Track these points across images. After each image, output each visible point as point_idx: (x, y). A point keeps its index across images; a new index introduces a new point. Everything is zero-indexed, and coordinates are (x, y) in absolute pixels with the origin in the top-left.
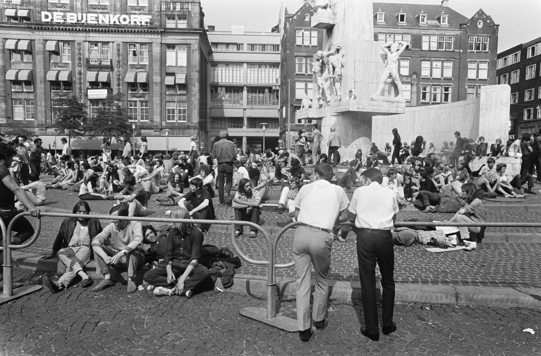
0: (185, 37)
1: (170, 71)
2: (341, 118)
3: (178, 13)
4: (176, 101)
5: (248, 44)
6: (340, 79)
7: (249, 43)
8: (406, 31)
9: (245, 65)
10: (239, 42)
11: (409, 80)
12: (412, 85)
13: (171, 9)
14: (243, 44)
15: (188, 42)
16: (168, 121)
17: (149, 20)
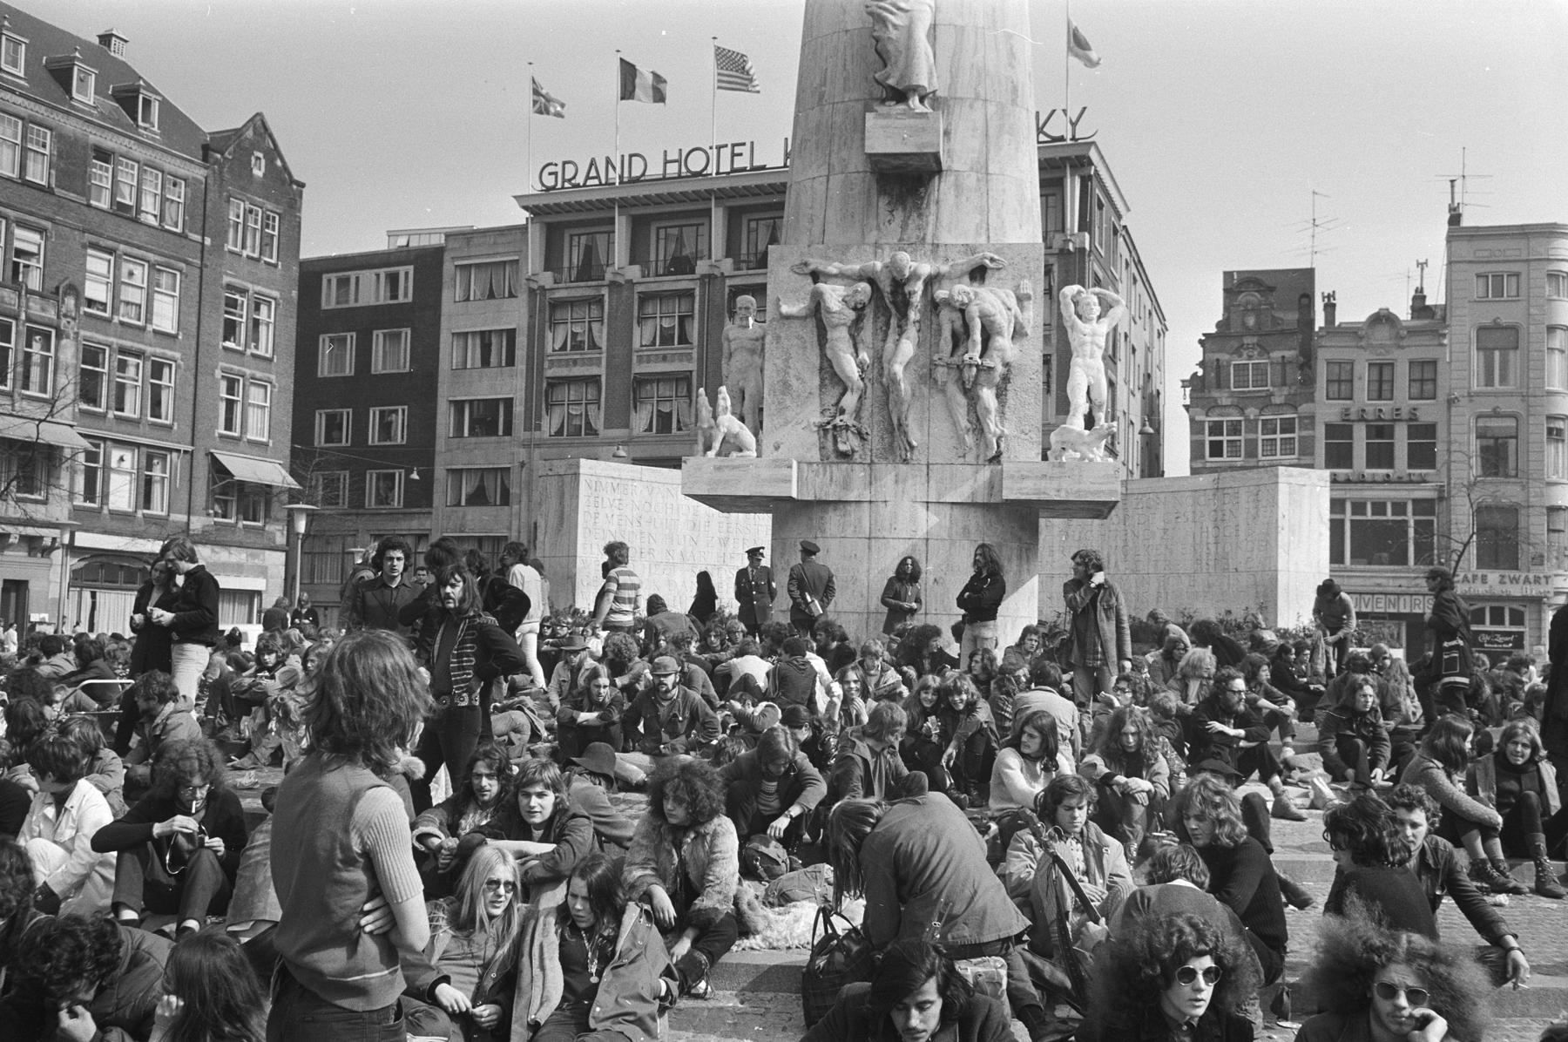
8: (40, 112)
11: (51, 314)
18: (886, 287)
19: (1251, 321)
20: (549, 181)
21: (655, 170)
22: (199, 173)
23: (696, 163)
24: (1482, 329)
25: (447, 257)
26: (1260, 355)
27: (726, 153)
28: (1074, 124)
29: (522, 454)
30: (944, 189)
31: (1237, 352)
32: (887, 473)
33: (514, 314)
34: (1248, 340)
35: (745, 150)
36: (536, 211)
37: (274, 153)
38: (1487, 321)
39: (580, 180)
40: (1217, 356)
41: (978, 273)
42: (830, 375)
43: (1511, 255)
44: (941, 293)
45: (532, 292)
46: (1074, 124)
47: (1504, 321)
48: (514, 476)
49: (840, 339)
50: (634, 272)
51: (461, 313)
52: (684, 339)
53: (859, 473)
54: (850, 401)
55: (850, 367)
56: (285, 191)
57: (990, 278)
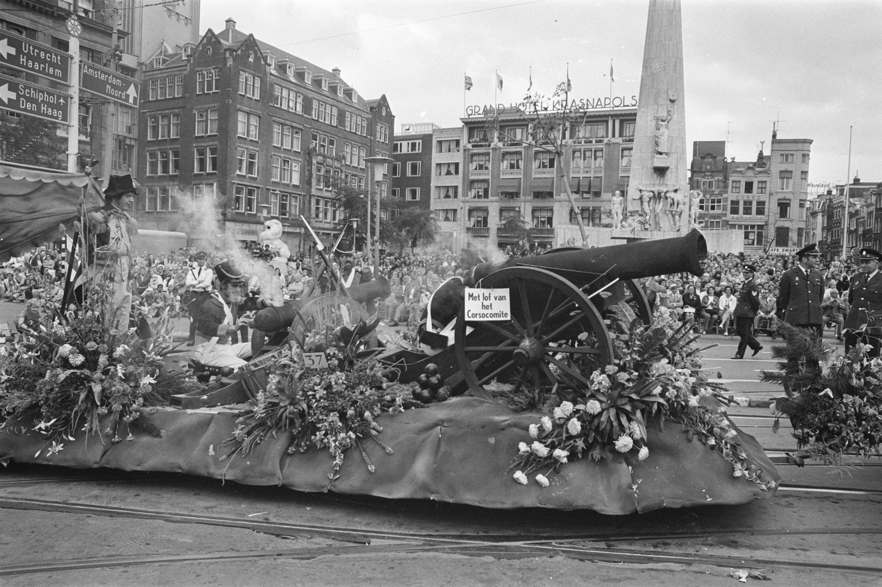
18: (656, 193)
19: (708, 167)
20: (470, 112)
22: (370, 116)
24: (781, 172)
25: (434, 137)
29: (462, 205)
30: (668, 173)
33: (457, 157)
36: (466, 123)
37: (388, 107)
38: (783, 169)
41: (676, 191)
43: (792, 148)
44: (668, 195)
45: (465, 150)
47: (789, 169)
48: (458, 212)
49: (646, 204)
50: (500, 145)
51: (437, 157)
52: (518, 167)
56: (390, 119)
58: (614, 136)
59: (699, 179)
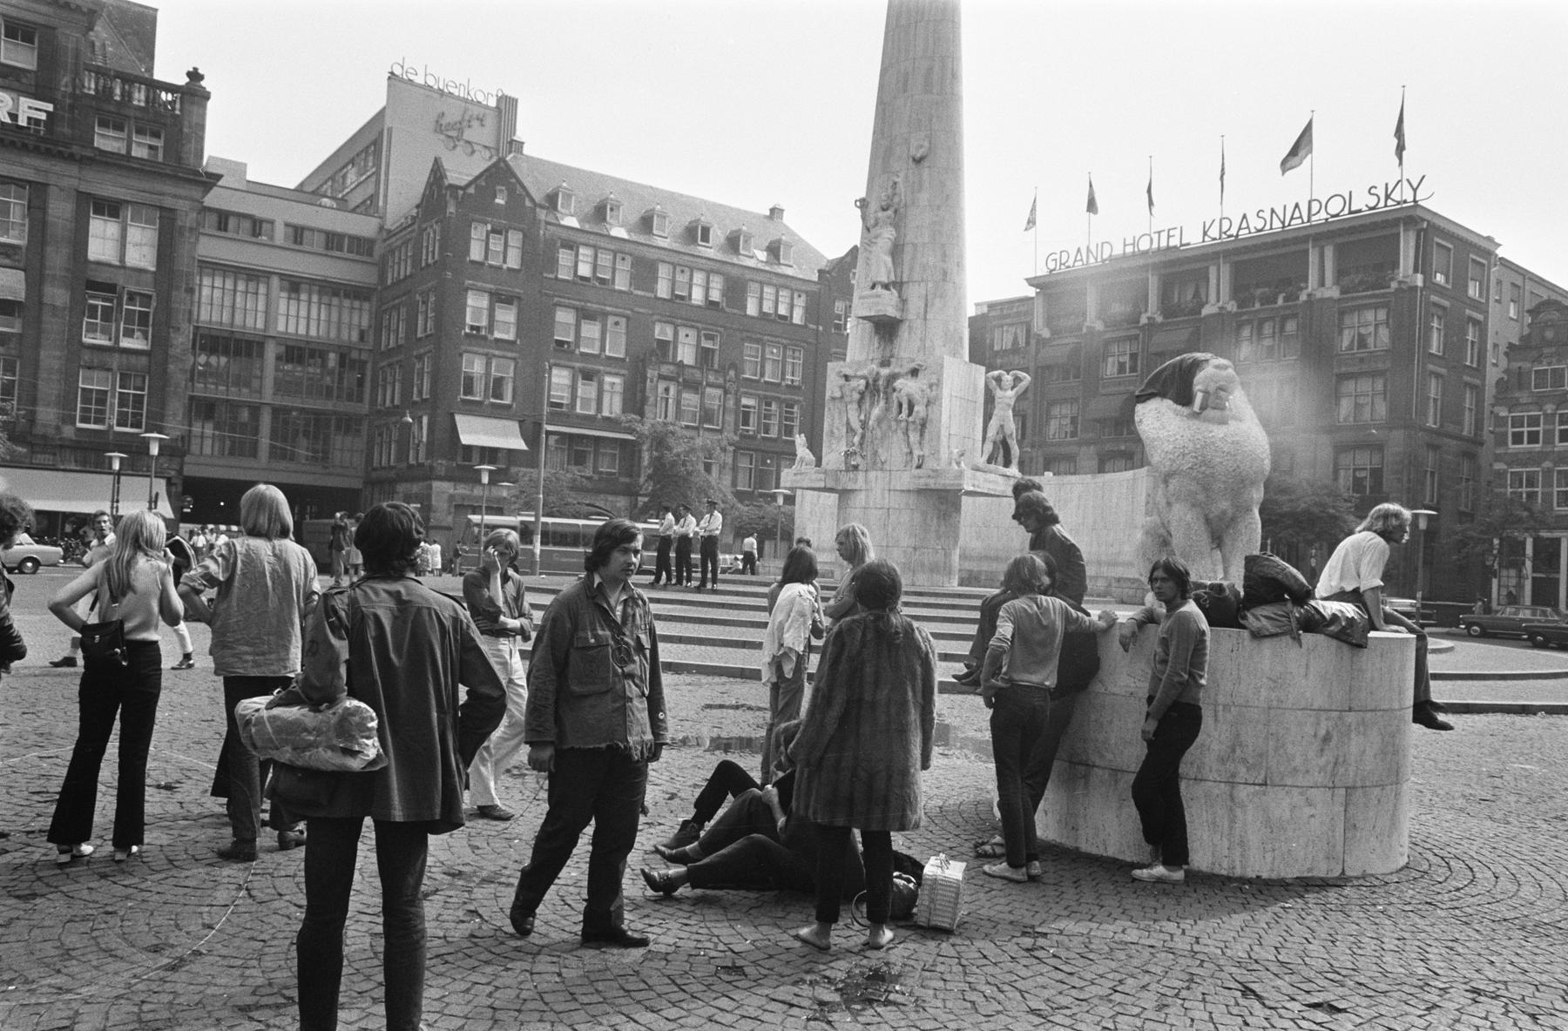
0: (159, 187)
1: (102, 276)
2: (912, 499)
3: (139, 114)
4: (115, 366)
5: (287, 225)
6: (923, 425)
7: (290, 221)
9: (275, 281)
10: (258, 212)
11: (721, 381)
12: (726, 392)
13: (117, 98)
14: (272, 222)
15: (168, 202)
16: (79, 425)
17: (43, 116)
21: (1118, 251)
23: (1144, 245)
26: (1559, 362)
27: (1164, 236)
28: (1415, 190)
31: (1538, 360)
32: (872, 474)
34: (1546, 351)
35: (1177, 233)
39: (1070, 263)
40: (1515, 365)
42: (850, 430)
46: (1415, 190)
53: (861, 475)
54: (856, 439)
55: (856, 425)
57: (920, 375)
58: (1322, 283)
59: (1526, 365)
